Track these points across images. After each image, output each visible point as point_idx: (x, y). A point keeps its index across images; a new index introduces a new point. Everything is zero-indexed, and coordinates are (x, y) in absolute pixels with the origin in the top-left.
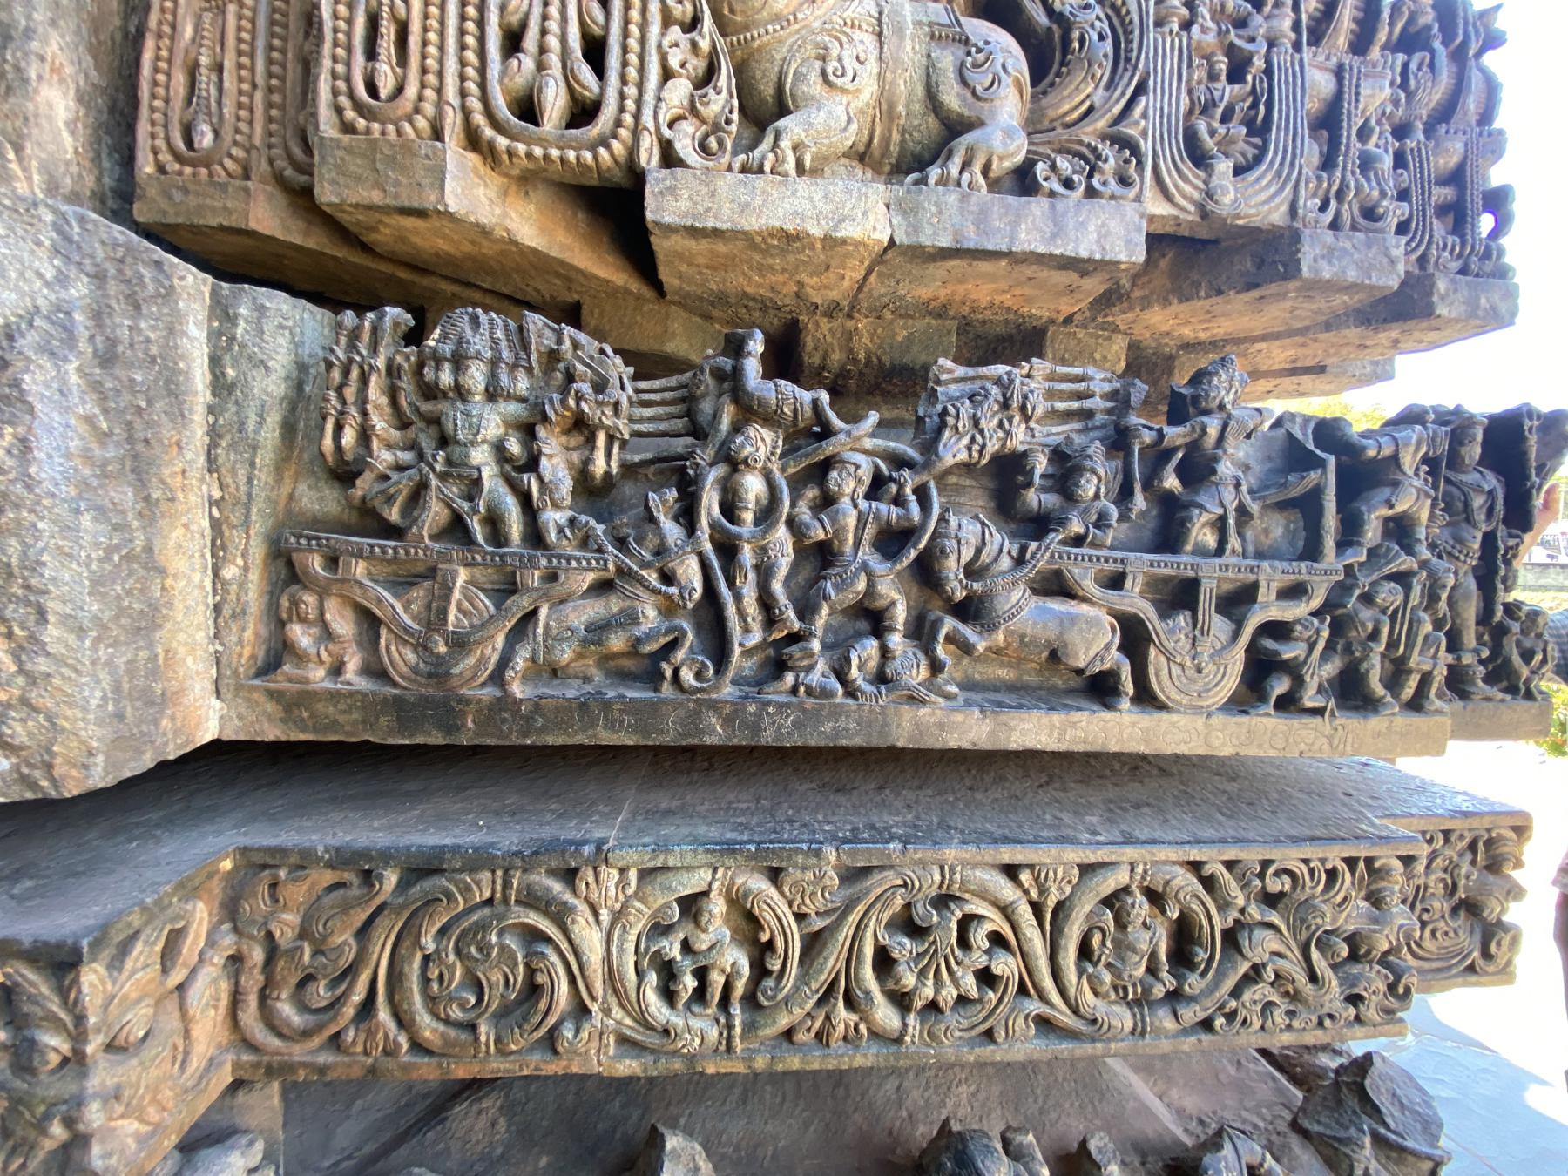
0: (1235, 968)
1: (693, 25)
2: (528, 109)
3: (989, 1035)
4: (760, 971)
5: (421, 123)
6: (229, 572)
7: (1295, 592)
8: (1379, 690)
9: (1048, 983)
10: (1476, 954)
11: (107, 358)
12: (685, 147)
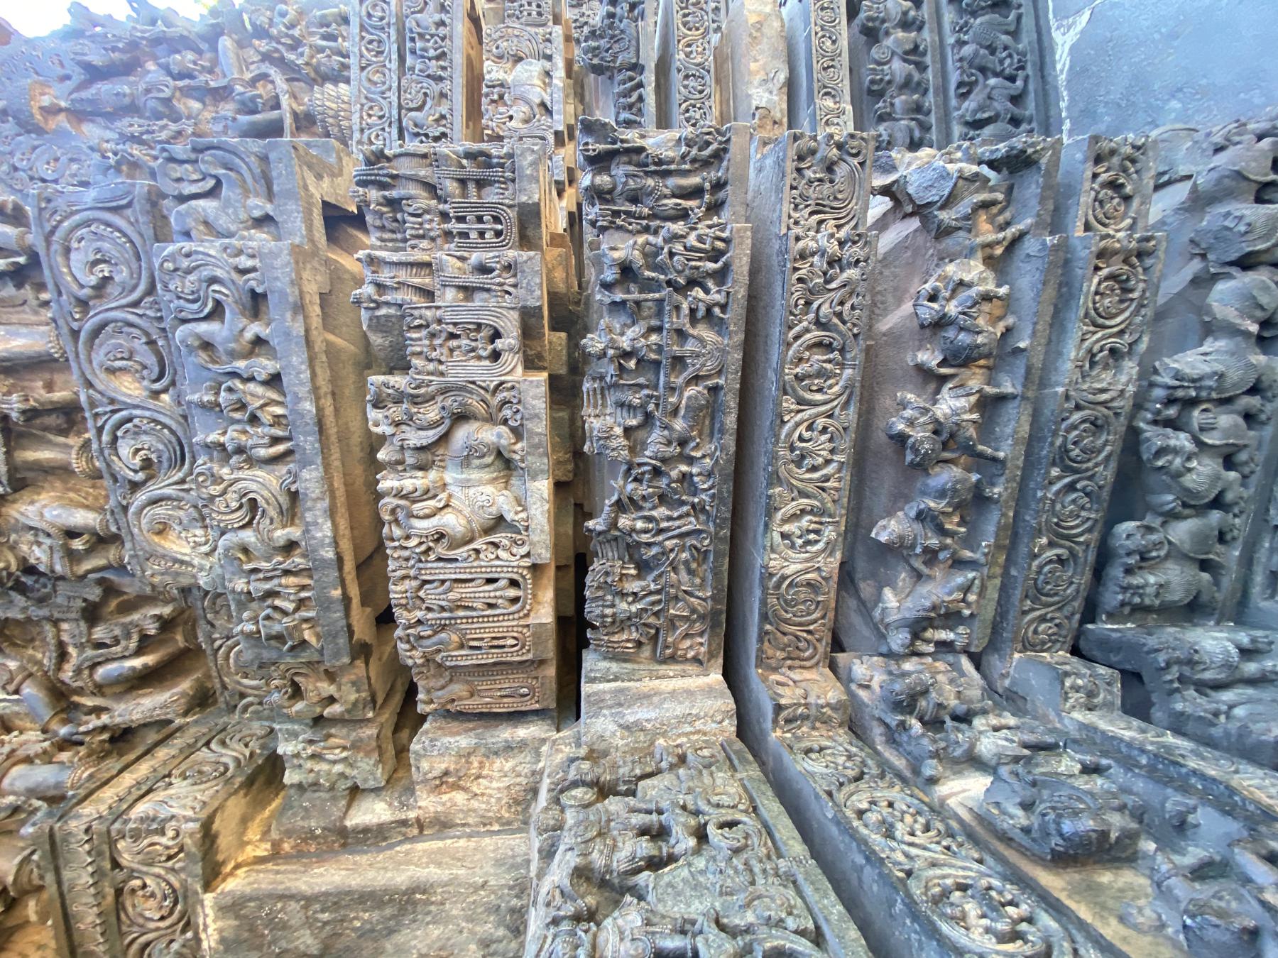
0: (836, 325)
1: (477, 551)
2: (515, 600)
3: (845, 429)
4: (811, 512)
5: (525, 630)
6: (671, 674)
7: (678, 308)
8: (720, 264)
9: (828, 407)
10: (855, 161)
11: (620, 705)
12: (523, 551)
